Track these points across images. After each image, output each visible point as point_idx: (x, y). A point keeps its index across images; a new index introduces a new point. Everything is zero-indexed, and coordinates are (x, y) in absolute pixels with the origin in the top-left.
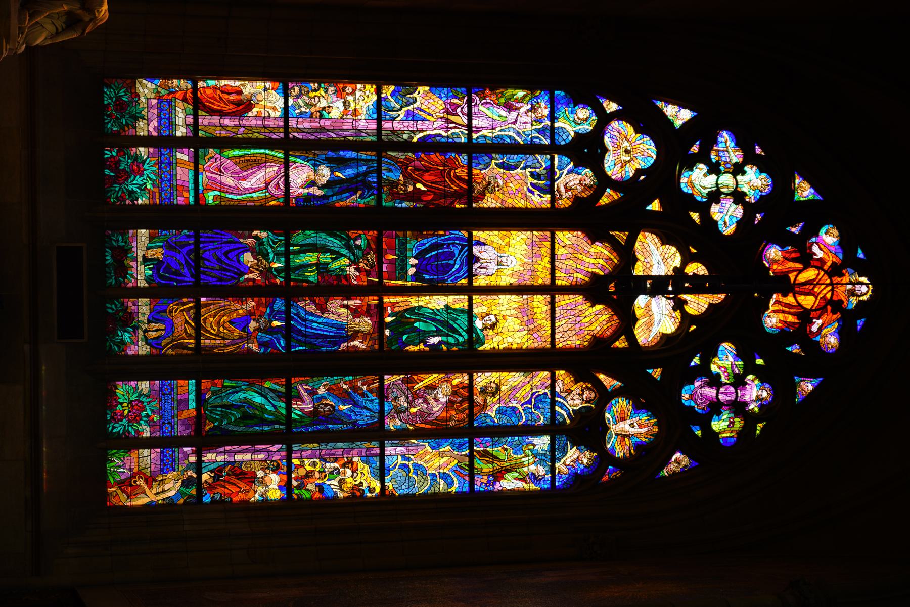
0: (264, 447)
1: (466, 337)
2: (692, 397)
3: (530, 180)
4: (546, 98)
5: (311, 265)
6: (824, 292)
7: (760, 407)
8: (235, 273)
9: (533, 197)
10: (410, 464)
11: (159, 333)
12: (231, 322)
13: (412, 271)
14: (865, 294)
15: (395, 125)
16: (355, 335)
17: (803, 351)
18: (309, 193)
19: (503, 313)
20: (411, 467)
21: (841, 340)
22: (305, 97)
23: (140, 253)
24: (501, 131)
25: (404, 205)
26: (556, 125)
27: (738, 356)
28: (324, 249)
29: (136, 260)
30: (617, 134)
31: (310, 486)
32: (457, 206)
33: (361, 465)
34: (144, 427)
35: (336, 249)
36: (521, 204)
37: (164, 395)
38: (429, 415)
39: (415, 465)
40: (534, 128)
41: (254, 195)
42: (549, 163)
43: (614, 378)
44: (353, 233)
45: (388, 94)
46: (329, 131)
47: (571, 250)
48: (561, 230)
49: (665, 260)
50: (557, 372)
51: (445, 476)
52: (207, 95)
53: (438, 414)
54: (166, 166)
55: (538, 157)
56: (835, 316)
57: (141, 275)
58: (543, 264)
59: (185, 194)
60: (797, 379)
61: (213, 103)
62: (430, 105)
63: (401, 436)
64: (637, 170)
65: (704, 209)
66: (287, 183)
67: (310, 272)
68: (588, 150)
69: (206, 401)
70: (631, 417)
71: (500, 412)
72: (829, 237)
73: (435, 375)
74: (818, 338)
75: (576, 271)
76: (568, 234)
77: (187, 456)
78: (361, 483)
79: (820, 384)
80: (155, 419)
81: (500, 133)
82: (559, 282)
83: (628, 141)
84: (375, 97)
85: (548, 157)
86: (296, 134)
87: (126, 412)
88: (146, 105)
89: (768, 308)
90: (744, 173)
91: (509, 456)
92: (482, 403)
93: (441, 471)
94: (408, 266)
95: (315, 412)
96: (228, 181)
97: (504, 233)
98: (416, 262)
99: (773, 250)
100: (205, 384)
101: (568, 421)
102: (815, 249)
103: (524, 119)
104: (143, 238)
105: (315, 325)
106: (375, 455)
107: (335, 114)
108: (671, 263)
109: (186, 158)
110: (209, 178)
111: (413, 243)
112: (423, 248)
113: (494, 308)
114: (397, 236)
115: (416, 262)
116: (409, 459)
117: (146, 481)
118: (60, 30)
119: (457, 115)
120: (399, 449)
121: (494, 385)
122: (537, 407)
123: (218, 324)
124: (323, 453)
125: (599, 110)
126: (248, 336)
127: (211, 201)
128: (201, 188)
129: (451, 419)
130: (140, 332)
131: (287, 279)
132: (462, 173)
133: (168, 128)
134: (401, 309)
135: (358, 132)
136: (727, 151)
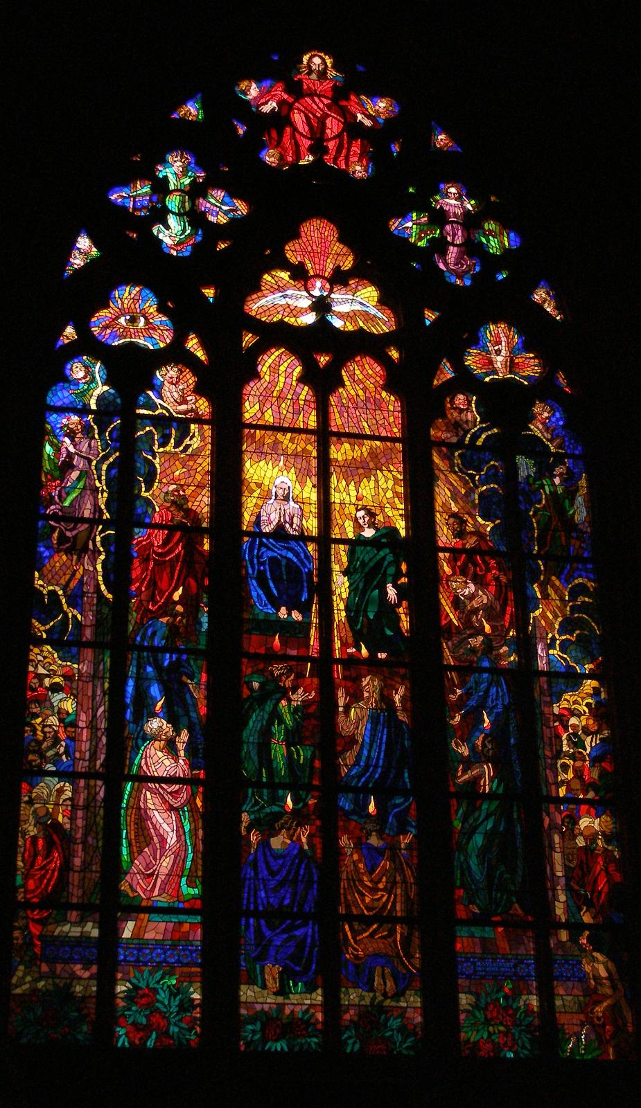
1: (387, 551)
2: (460, 276)
4: (55, 416)
5: (290, 754)
6: (321, 106)
7: (470, 197)
8: (301, 861)
9: (195, 446)
10: (559, 638)
12: (371, 871)
13: (296, 616)
14: (323, 60)
15: (89, 623)
16: (385, 698)
19: (354, 500)
20: (564, 637)
21: (382, 96)
23: (271, 999)
24: (101, 483)
26: (94, 407)
27: (404, 215)
28: (266, 734)
29: (281, 1007)
30: (108, 331)
32: (206, 547)
33: (564, 704)
34: (522, 1003)
35: (266, 716)
36: (205, 463)
37: (475, 971)
40: (97, 436)
41: (187, 828)
42: (148, 422)
44: (246, 693)
45: (42, 628)
49: (280, 289)
51: (574, 593)
52: (37, 888)
57: (305, 1000)
58: (286, 442)
61: (49, 880)
62: (61, 573)
64: (159, 310)
66: (171, 780)
67: (299, 756)
68: (132, 370)
70: (488, 352)
74: (381, 121)
75: (295, 401)
77: (560, 944)
80: (510, 986)
81: (104, 482)
82: (312, 423)
83: (118, 318)
85: (139, 421)
86: (98, 763)
87: (501, 1028)
88: (50, 981)
90: (166, 178)
92: (474, 538)
93: (567, 598)
94: (290, 619)
96: (166, 863)
99: (267, 158)
100: (461, 913)
102: (266, 109)
105: (374, 754)
107: (69, 706)
108: (284, 282)
109: (131, 925)
111: (257, 611)
112: (264, 599)
113: (347, 511)
116: (553, 639)
119: (75, 537)
120: (539, 651)
121: (451, 520)
122: (479, 470)
123: (374, 890)
124: (548, 753)
125: (74, 351)
126: (393, 848)
127: (196, 891)
129: (497, 579)
130: (388, 1002)
131: (309, 788)
132: (159, 537)
134: (350, 634)
135: (95, 677)
136: (134, 197)
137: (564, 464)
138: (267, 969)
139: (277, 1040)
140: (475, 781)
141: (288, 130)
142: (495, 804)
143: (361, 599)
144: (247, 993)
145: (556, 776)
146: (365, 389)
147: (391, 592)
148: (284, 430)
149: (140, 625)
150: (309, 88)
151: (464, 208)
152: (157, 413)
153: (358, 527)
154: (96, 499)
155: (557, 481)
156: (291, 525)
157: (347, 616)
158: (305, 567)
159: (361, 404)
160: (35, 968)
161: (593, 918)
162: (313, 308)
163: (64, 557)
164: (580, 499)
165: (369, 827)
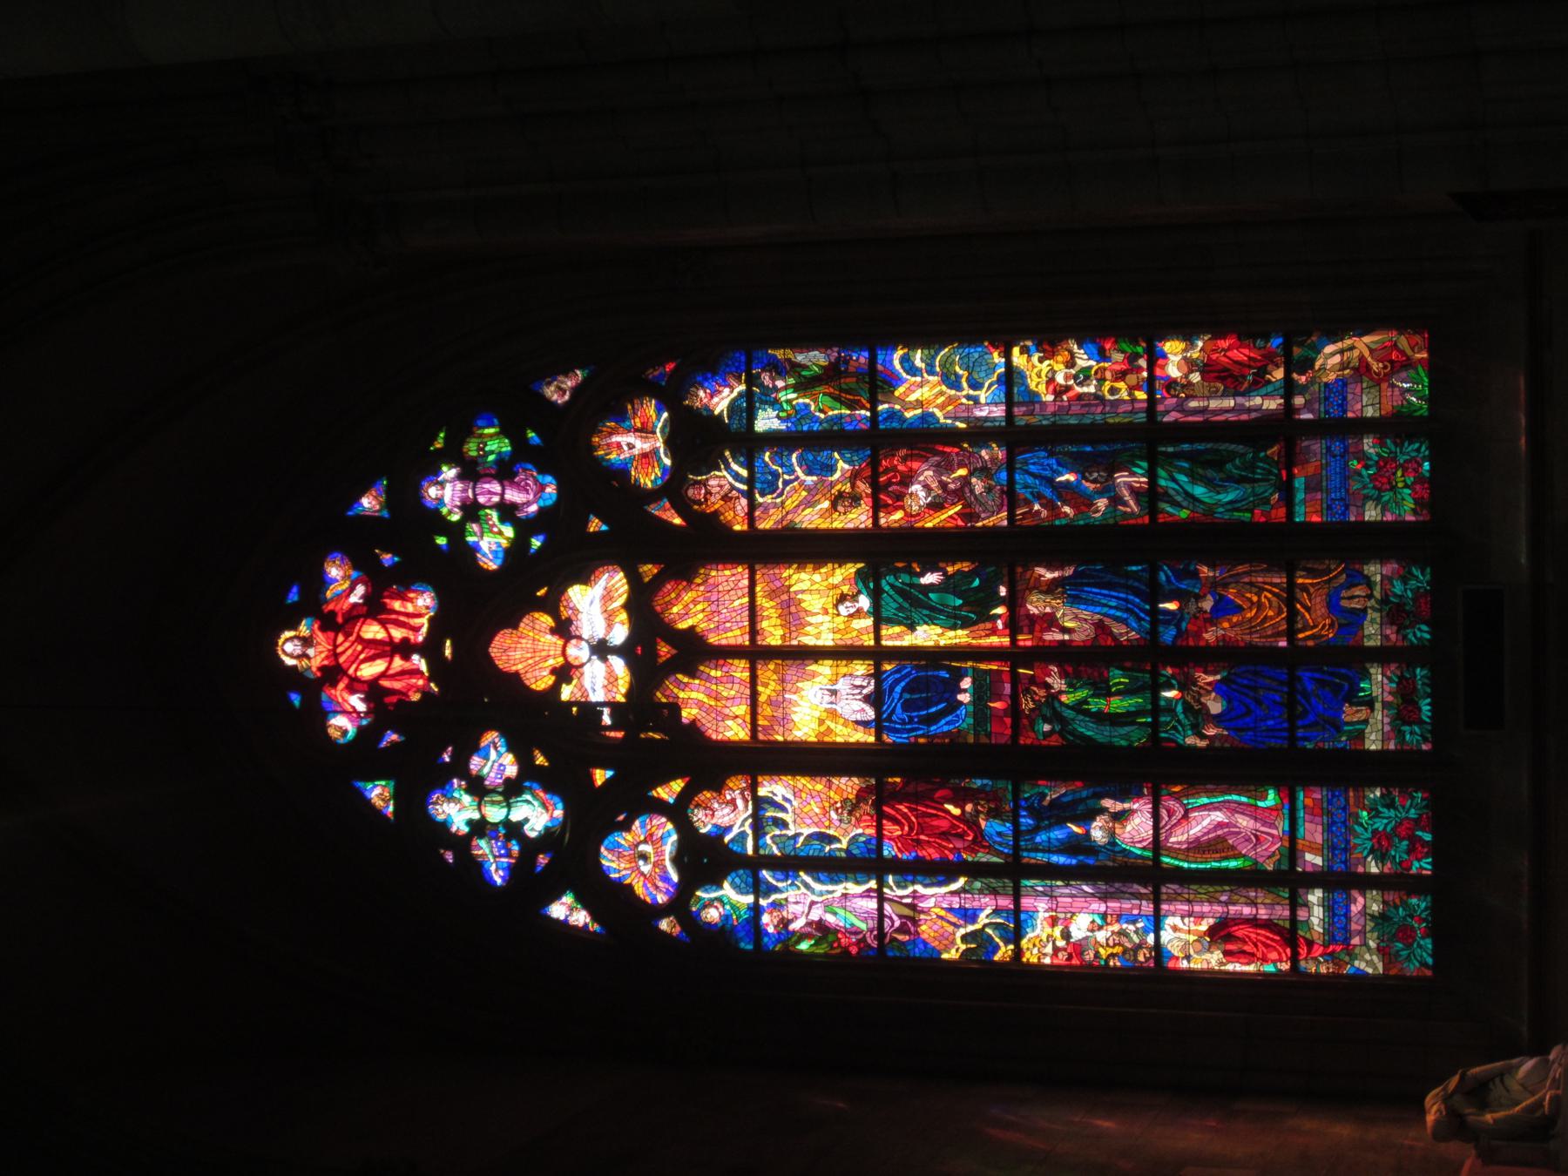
0: (1190, 419)
2: (542, 488)
3: (788, 817)
4: (766, 939)
5: (1118, 693)
7: (438, 472)
10: (967, 391)
11: (1349, 593)
13: (966, 683)
14: (287, 640)
16: (1051, 588)
17: (377, 556)
18: (1123, 801)
19: (828, 618)
20: (965, 385)
22: (1129, 945)
25: (979, 782)
26: (750, 899)
27: (476, 548)
28: (1101, 718)
29: (1385, 705)
30: (660, 884)
31: (1119, 357)
33: (1042, 388)
36: (803, 781)
38: (938, 465)
39: (959, 388)
41: (1205, 800)
43: (659, 519)
44: (1055, 741)
45: (1003, 949)
46: (1093, 895)
47: (727, 711)
48: (741, 742)
50: (745, 527)
51: (913, 371)
53: (924, 467)
54: (1337, 846)
55: (777, 852)
56: (331, 607)
57: (1377, 682)
58: (768, 692)
59: (1309, 802)
60: (385, 514)
63: (980, 433)
64: (628, 829)
65: (527, 769)
66: (1156, 816)
68: (705, 859)
69: (1278, 489)
70: (632, 458)
71: (831, 469)
72: (342, 725)
73: (929, 525)
74: (355, 574)
75: (718, 681)
76: (729, 735)
77: (1308, 406)
78: (1041, 360)
79: (350, 507)
82: (743, 664)
83: (642, 874)
84: (1024, 943)
86: (1143, 891)
87: (1399, 473)
89: (431, 620)
90: (470, 823)
91: (816, 402)
92: (859, 483)
93: (918, 379)
95: (1112, 470)
96: (1244, 822)
97: (827, 739)
98: (961, 697)
101: (727, 453)
103: (798, 909)
104: (1373, 737)
106: (1020, 404)
109: (1309, 857)
110: (1272, 826)
112: (949, 718)
114: (988, 735)
115: (961, 697)
116: (968, 397)
117: (1368, 367)
118: (1497, 1080)
119: (900, 917)
121: (840, 508)
122: (776, 476)
123: (1260, 606)
124: (1100, 409)
125: (689, 921)
126: (1214, 586)
128: (1286, 811)
130: (1377, 594)
131: (1155, 674)
133: (1335, 902)
134: (982, 626)
137: (759, 374)
138: (1347, 719)
139: (1420, 710)
140: (1135, 492)
141: (386, 683)
142: (1162, 473)
143: (941, 612)
144: (1373, 743)
145: (1124, 401)
146: (695, 602)
147: (930, 578)
148: (754, 695)
149: (990, 849)
150: (327, 658)
151: (452, 481)
152: (749, 832)
153: (858, 613)
154: (854, 896)
155: (780, 384)
156: (863, 687)
157: (962, 627)
158: (909, 674)
159: (714, 607)
160: (1357, 951)
161: (1278, 367)
162: (604, 659)
163: (924, 928)
164: (800, 358)
165: (1192, 608)
